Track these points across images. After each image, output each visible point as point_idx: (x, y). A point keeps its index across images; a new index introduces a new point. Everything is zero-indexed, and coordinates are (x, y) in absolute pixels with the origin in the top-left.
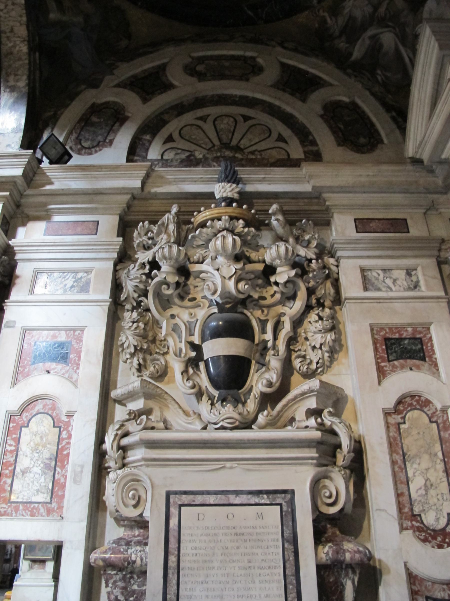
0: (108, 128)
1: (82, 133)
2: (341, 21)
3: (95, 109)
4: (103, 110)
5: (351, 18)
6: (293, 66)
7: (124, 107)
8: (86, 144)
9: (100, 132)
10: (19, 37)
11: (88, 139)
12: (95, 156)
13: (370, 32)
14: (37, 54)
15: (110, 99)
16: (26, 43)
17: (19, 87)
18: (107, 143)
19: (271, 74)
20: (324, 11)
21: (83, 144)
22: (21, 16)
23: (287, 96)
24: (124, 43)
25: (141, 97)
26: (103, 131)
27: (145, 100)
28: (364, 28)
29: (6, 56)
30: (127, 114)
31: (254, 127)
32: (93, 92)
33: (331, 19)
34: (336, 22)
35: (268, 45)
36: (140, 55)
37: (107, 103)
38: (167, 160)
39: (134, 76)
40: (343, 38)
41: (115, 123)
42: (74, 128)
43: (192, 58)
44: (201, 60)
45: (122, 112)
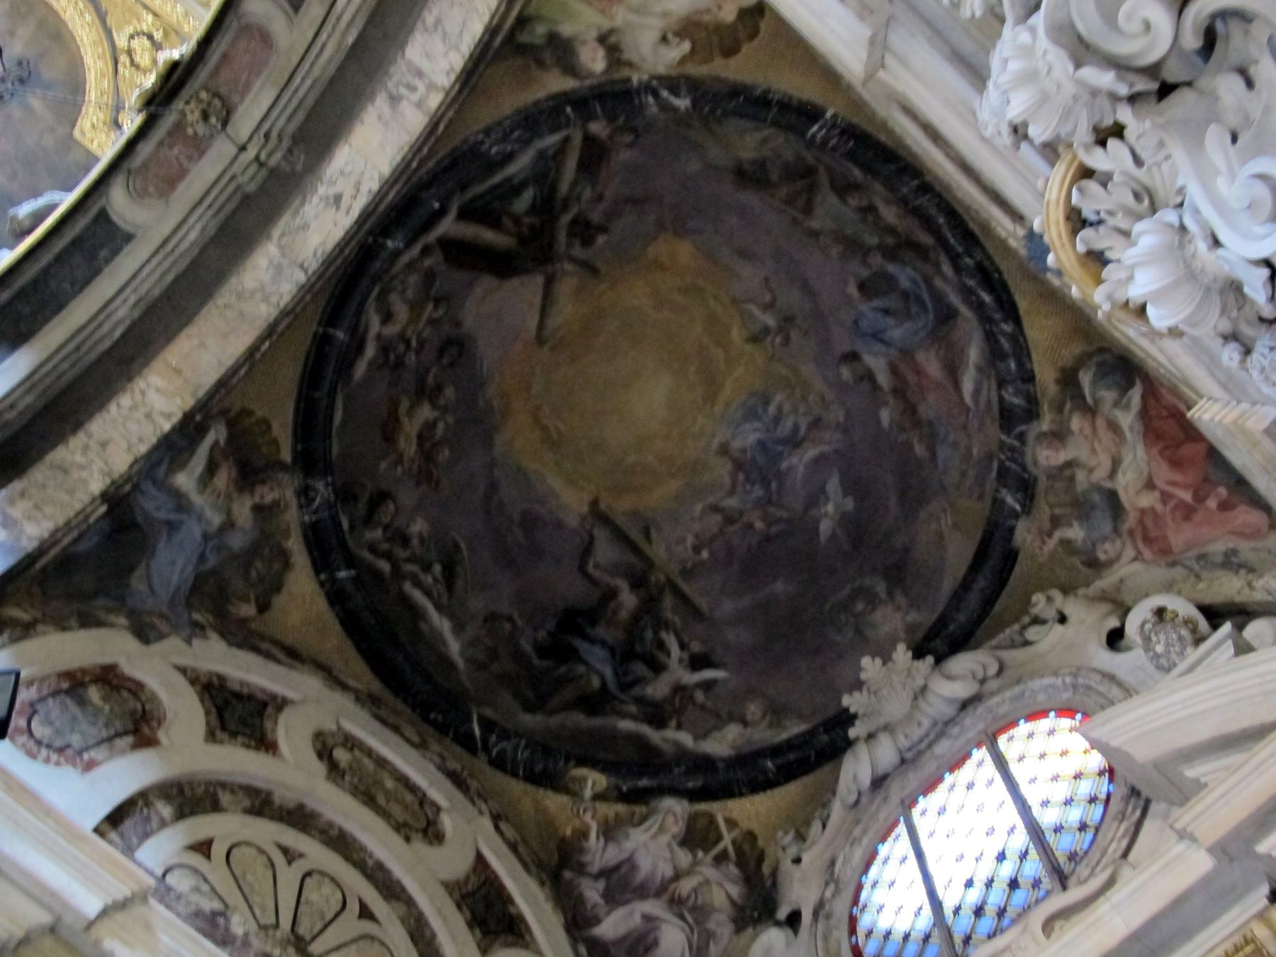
0: (105, 734)
1: (50, 701)
2: (613, 855)
3: (108, 677)
5: (630, 863)
6: (493, 872)
9: (84, 726)
10: (106, 463)
11: (51, 723)
13: (651, 907)
17: (22, 531)
19: (452, 861)
20: (593, 817)
22: (141, 440)
23: (459, 921)
24: (247, 610)
25: (208, 723)
26: (94, 731)
27: (211, 736)
28: (642, 892)
29: (53, 466)
31: (369, 942)
33: (598, 838)
34: (604, 850)
35: (474, 804)
38: (169, 889)
40: (601, 885)
41: (126, 733)
42: (42, 680)
43: (339, 728)
44: (350, 743)
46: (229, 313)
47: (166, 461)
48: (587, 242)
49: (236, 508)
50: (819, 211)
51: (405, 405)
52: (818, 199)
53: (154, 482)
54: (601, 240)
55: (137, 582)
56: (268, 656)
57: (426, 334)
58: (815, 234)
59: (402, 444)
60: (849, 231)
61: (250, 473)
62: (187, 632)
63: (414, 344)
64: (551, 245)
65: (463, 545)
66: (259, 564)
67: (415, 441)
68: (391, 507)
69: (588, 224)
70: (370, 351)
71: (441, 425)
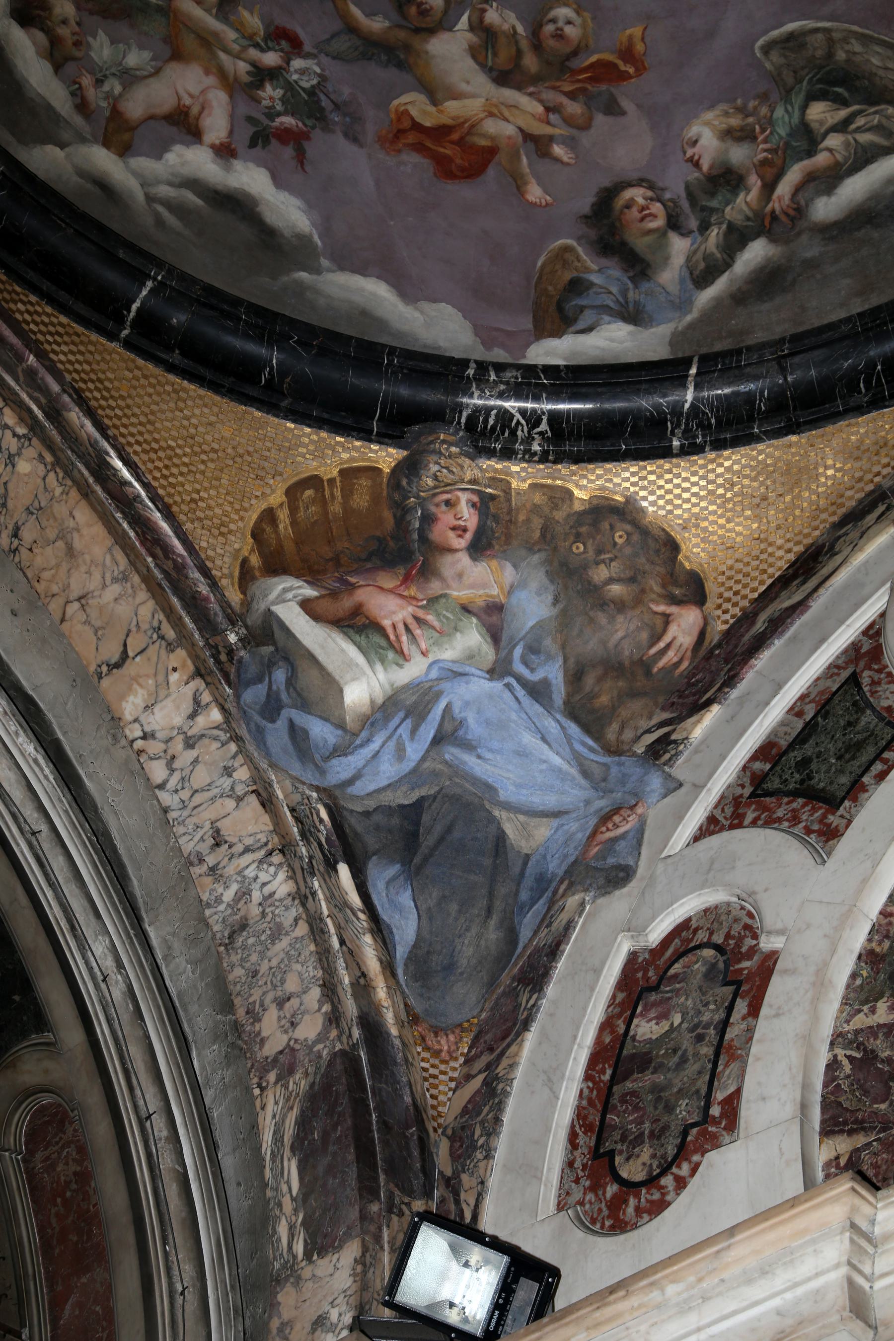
4: (677, 968)
7: (750, 915)
8: (632, 1170)
10: (247, 850)
11: (639, 1140)
12: (680, 1205)
14: (344, 870)
15: (687, 907)
16: (277, 858)
18: (715, 1122)
21: (624, 1174)
30: (767, 943)
32: (618, 904)
36: (760, 643)
37: (684, 926)
39: (764, 751)
45: (749, 942)
46: (28, 534)
47: (302, 719)
49: (459, 593)
51: (415, 104)
53: (340, 751)
55: (529, 837)
56: (777, 625)
57: (253, 21)
59: (503, 130)
61: (401, 547)
62: (655, 782)
63: (271, 59)
65: (791, 27)
66: (600, 574)
67: (509, 94)
68: (637, 194)
70: (251, 178)
71: (492, 16)
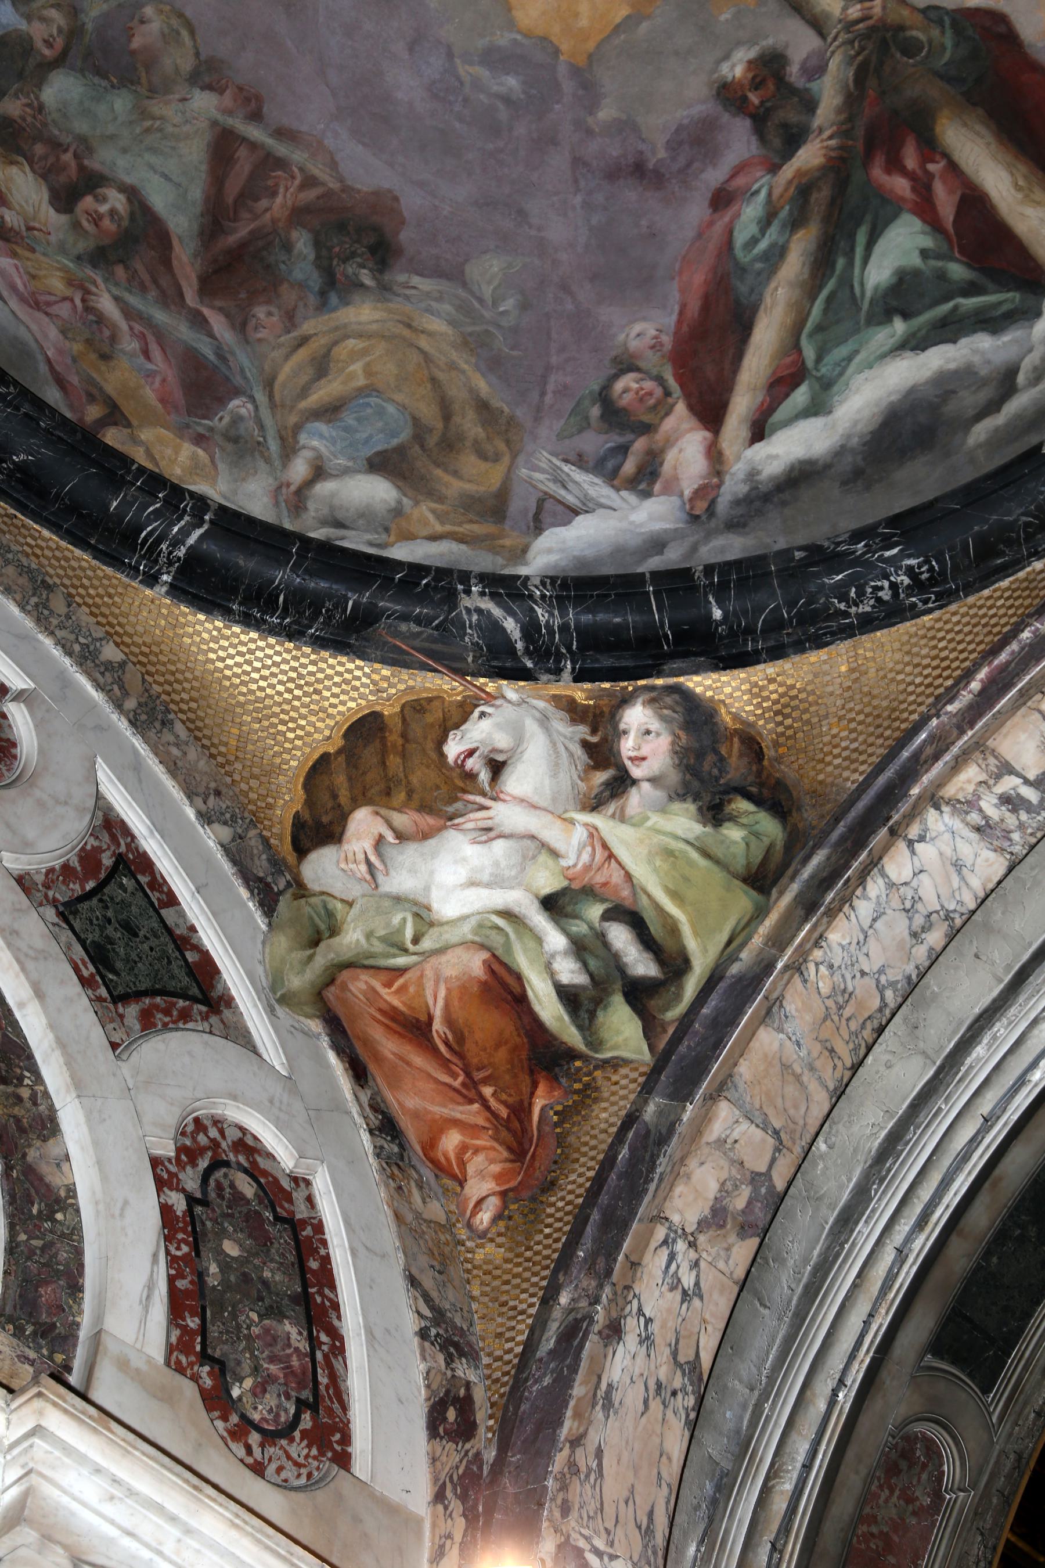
48: (770, 66)
50: (195, 152)
52: (197, 193)
54: (736, 68)
58: (208, 74)
60: (121, 103)
64: (860, 78)
69: (760, 121)
